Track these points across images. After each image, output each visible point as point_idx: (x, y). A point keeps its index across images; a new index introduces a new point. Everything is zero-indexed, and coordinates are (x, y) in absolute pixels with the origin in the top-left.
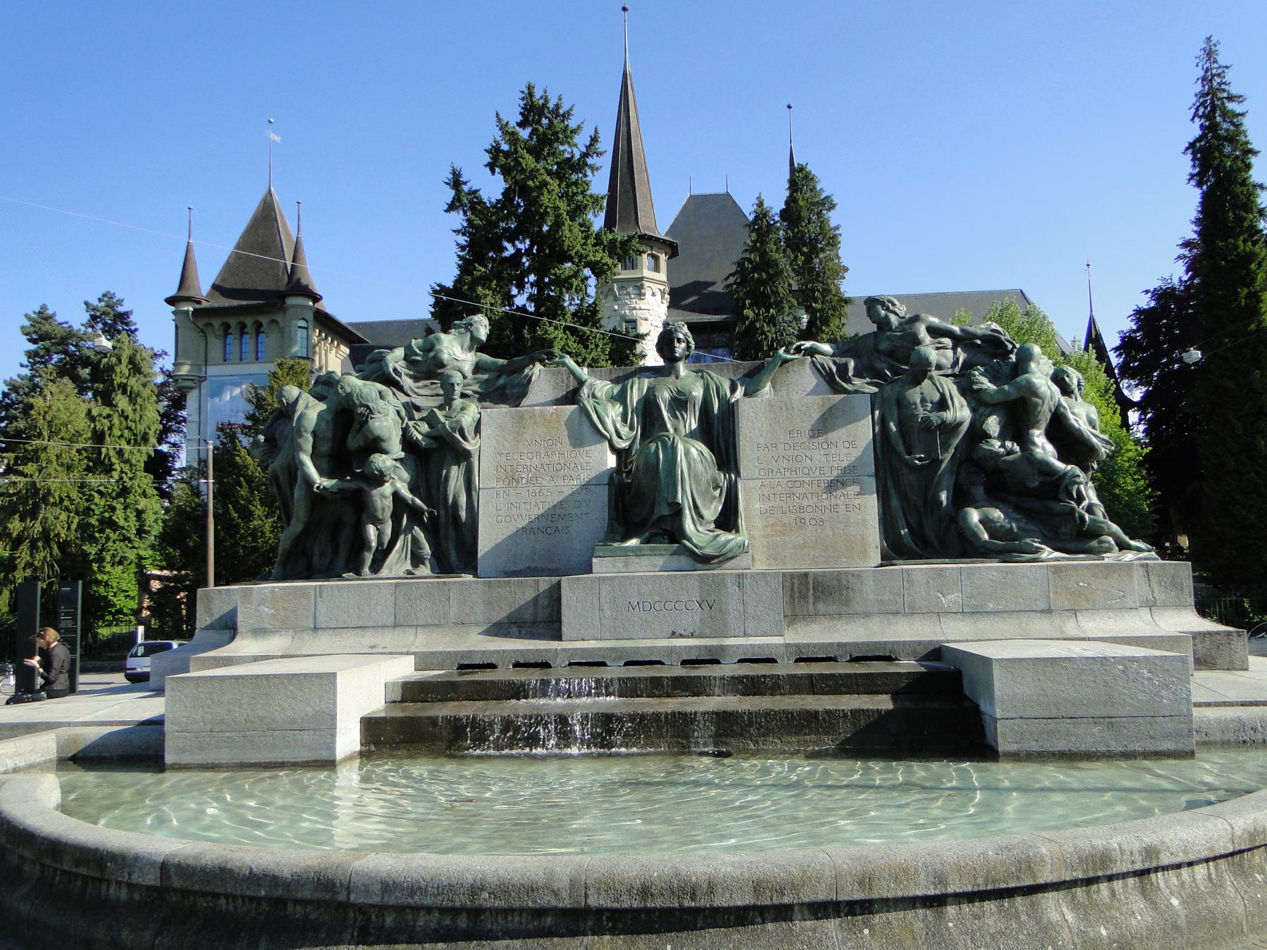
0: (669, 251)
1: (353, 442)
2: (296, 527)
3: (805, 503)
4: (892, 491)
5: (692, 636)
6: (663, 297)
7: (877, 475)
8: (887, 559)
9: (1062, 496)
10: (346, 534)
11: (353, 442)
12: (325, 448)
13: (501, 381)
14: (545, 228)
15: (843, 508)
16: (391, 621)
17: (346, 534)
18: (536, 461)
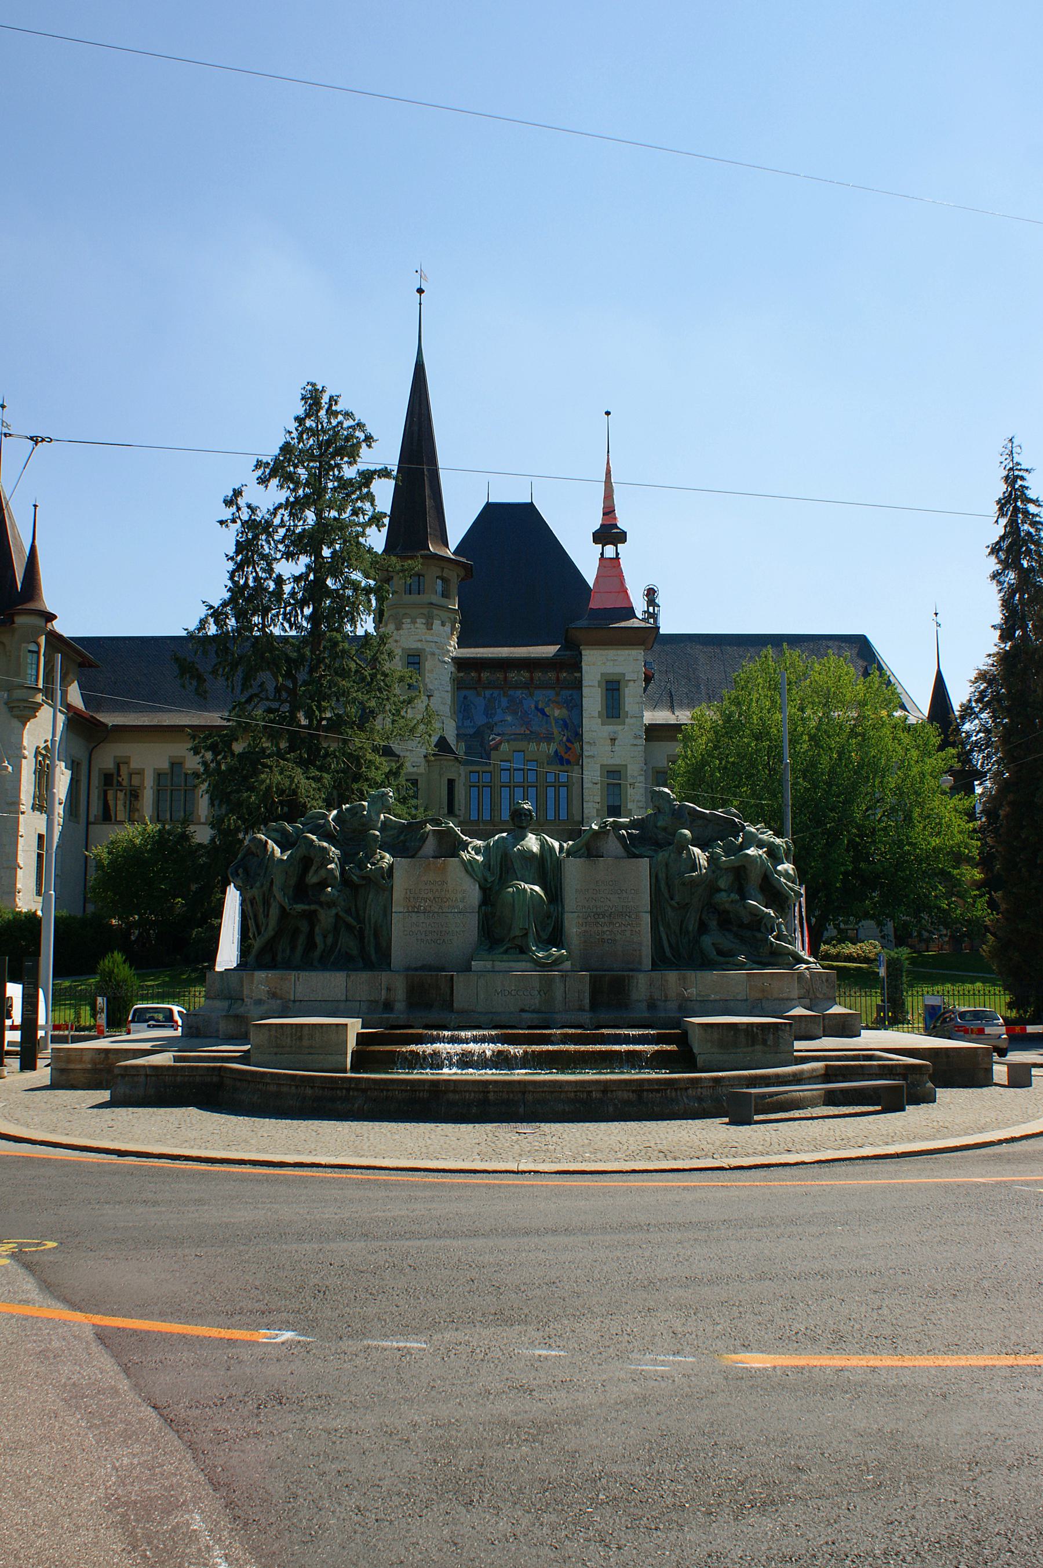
0: (462, 573)
1: (312, 879)
2: (270, 932)
3: (606, 929)
4: (660, 923)
5: (533, 1011)
6: (453, 628)
7: (651, 912)
8: (655, 966)
9: (763, 930)
10: (302, 940)
11: (312, 879)
12: (292, 882)
13: (402, 838)
14: (505, 834)
15: (628, 933)
16: (344, 998)
17: (302, 940)
18: (430, 895)
